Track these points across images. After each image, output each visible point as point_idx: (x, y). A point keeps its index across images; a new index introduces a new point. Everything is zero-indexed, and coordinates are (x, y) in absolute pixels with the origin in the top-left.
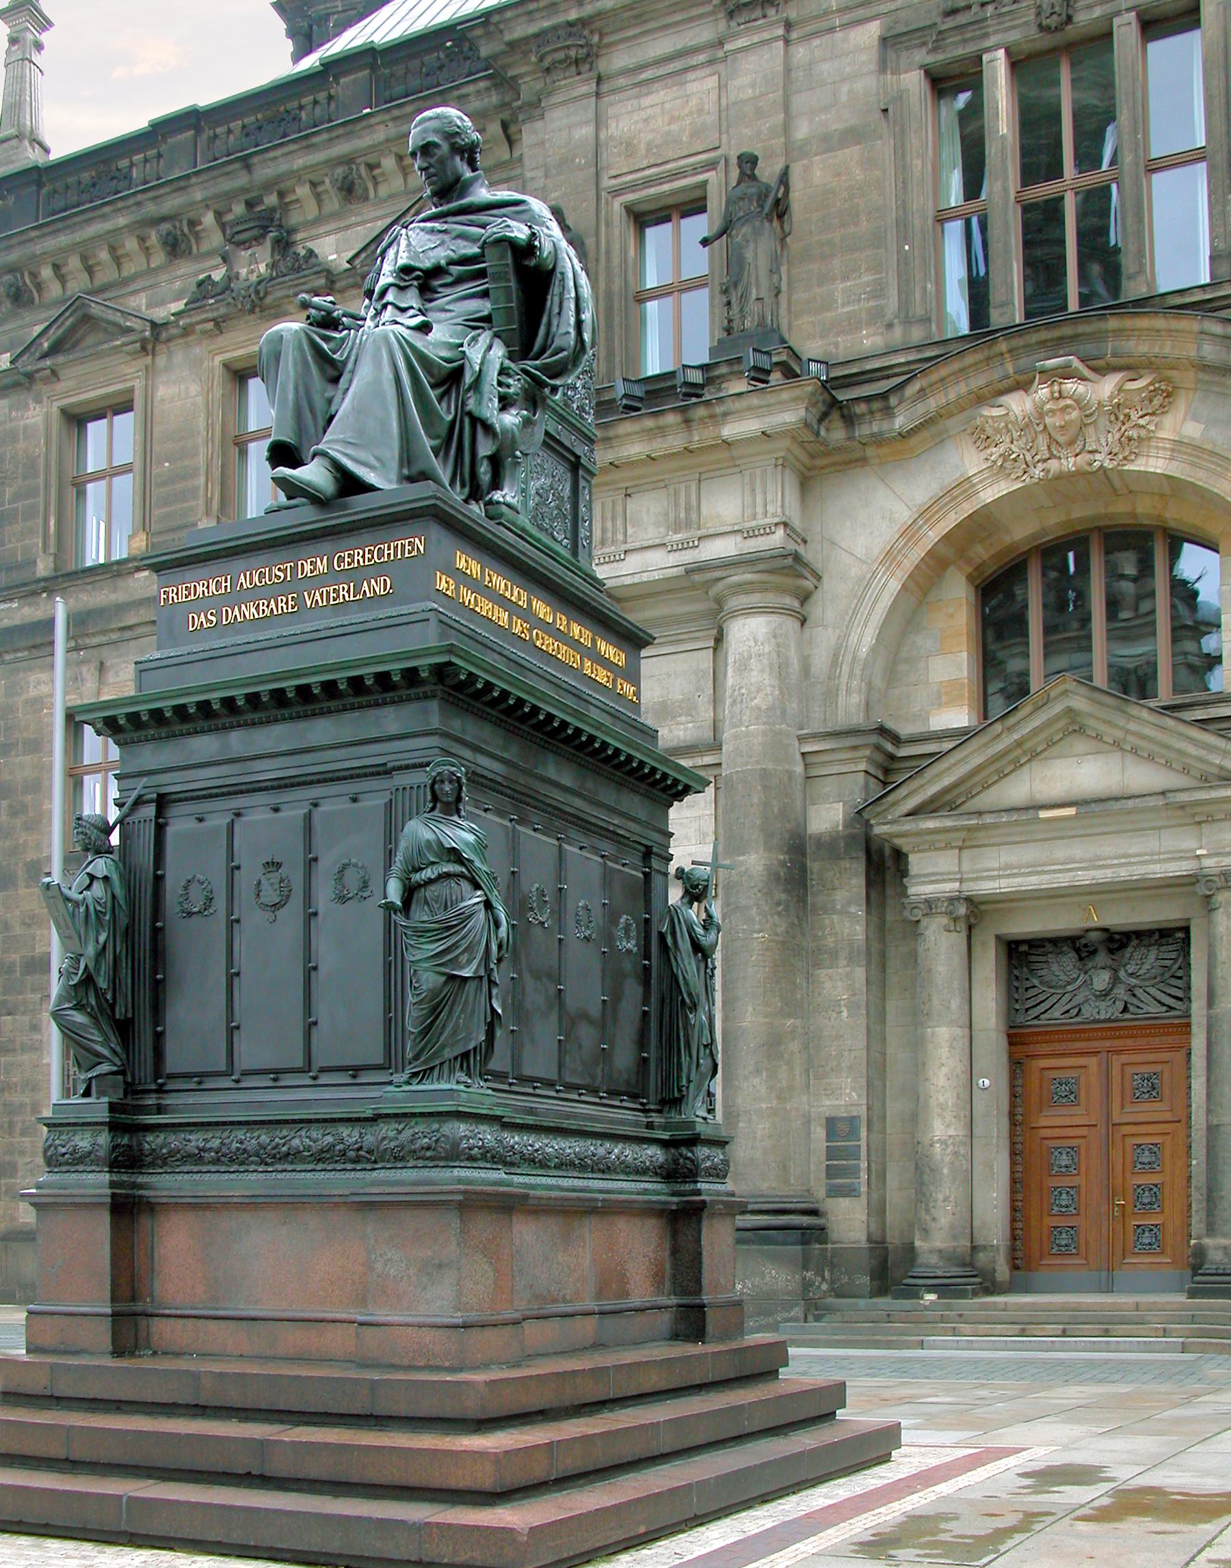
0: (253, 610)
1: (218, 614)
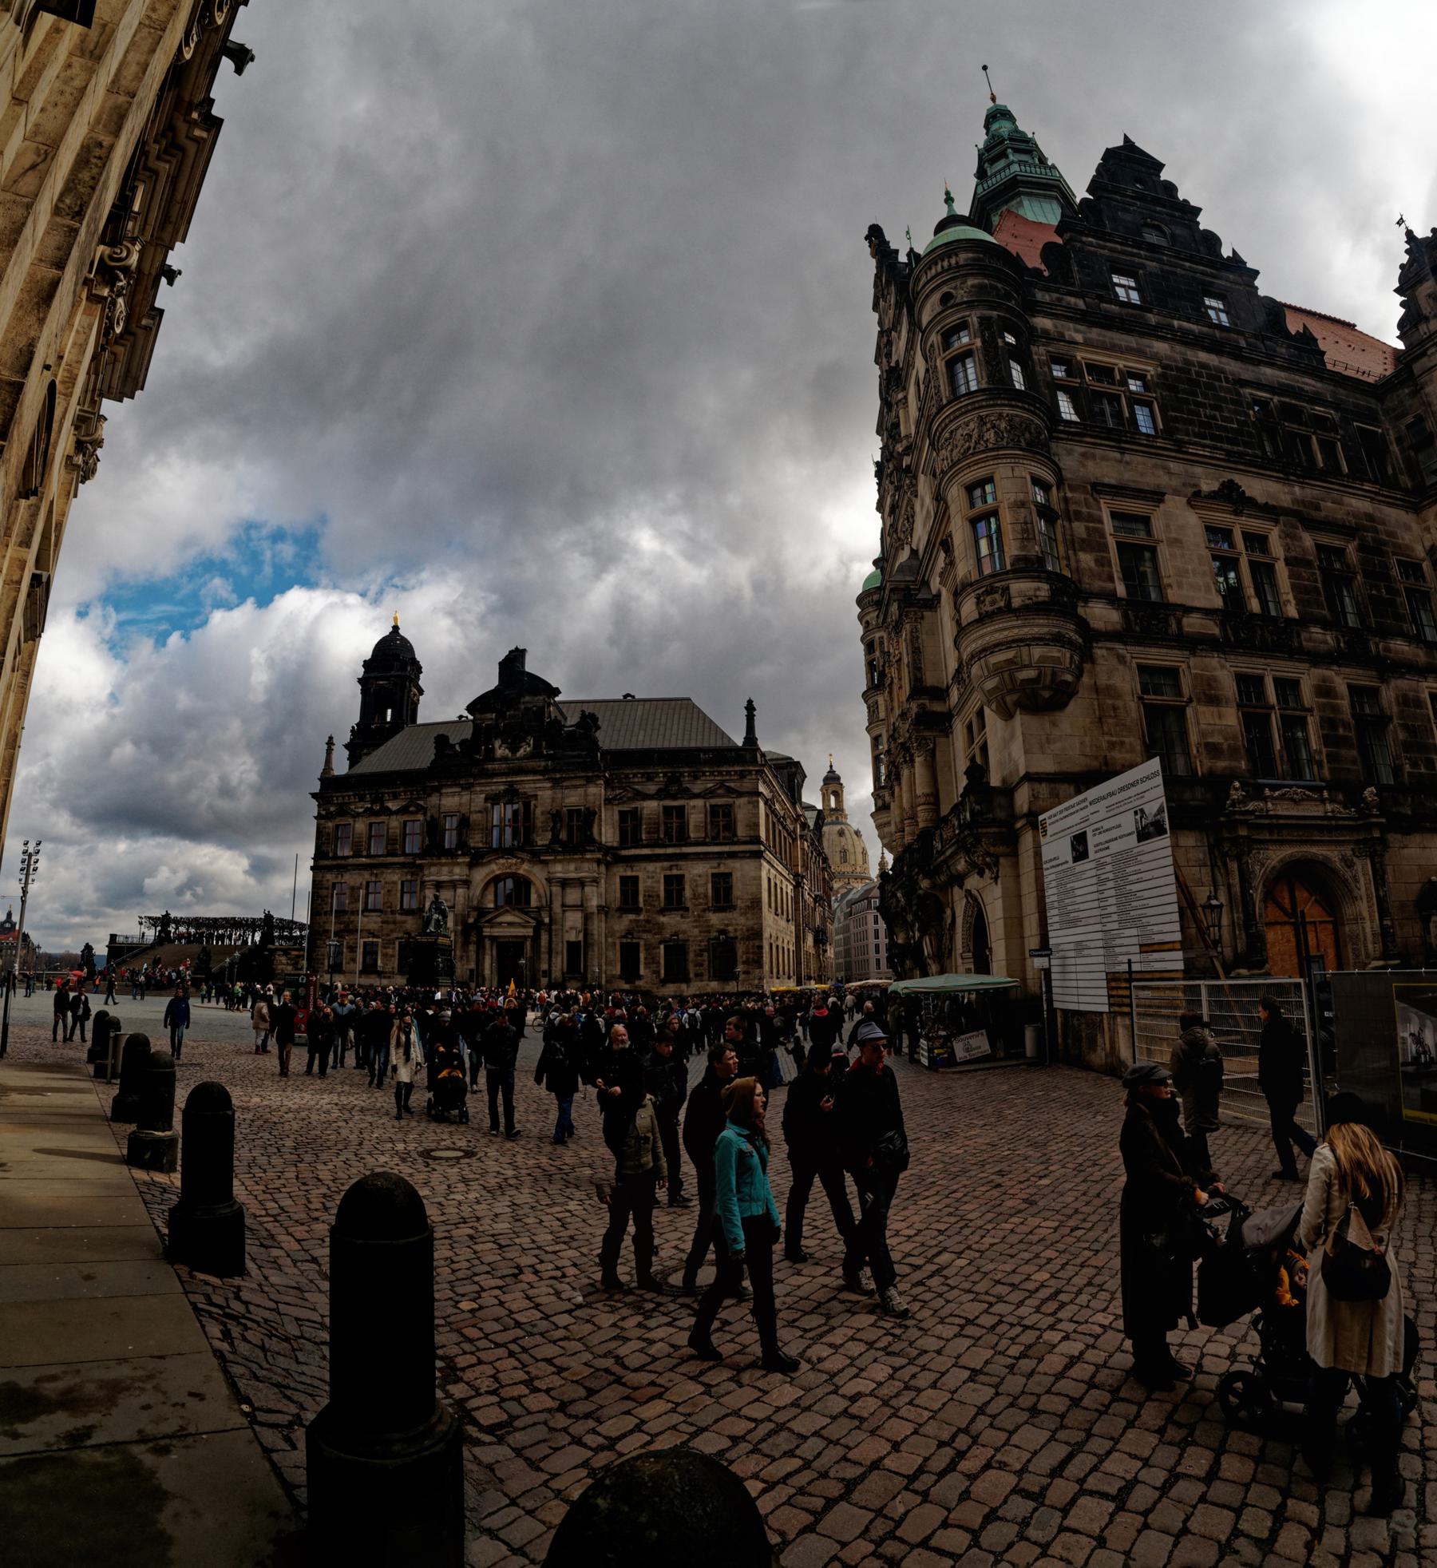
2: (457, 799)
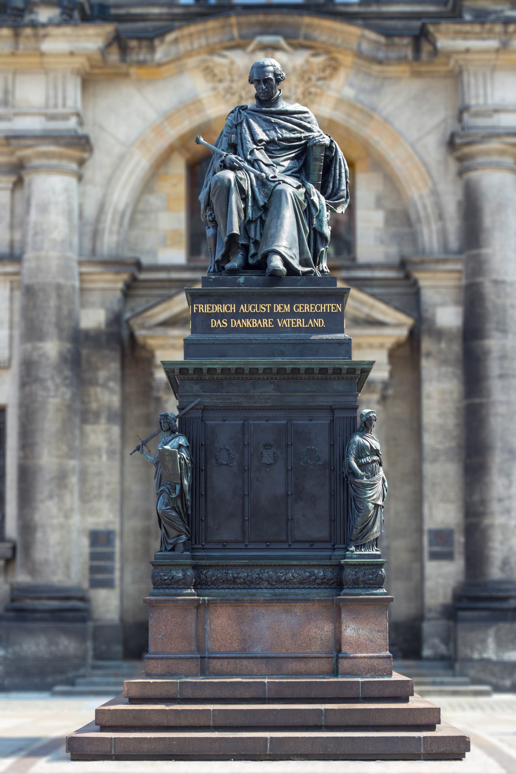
0: (248, 323)
1: (229, 322)
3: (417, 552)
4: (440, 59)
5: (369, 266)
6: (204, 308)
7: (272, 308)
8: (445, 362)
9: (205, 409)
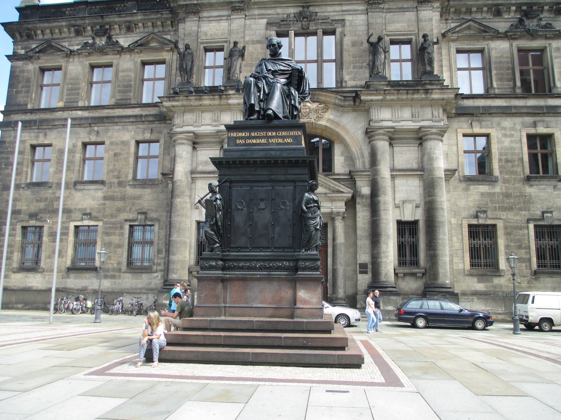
1: (245, 141)
2: (224, 24)
3: (355, 271)
4: (363, 105)
5: (338, 174)
6: (234, 134)
7: (266, 134)
8: (365, 206)
9: (231, 182)
